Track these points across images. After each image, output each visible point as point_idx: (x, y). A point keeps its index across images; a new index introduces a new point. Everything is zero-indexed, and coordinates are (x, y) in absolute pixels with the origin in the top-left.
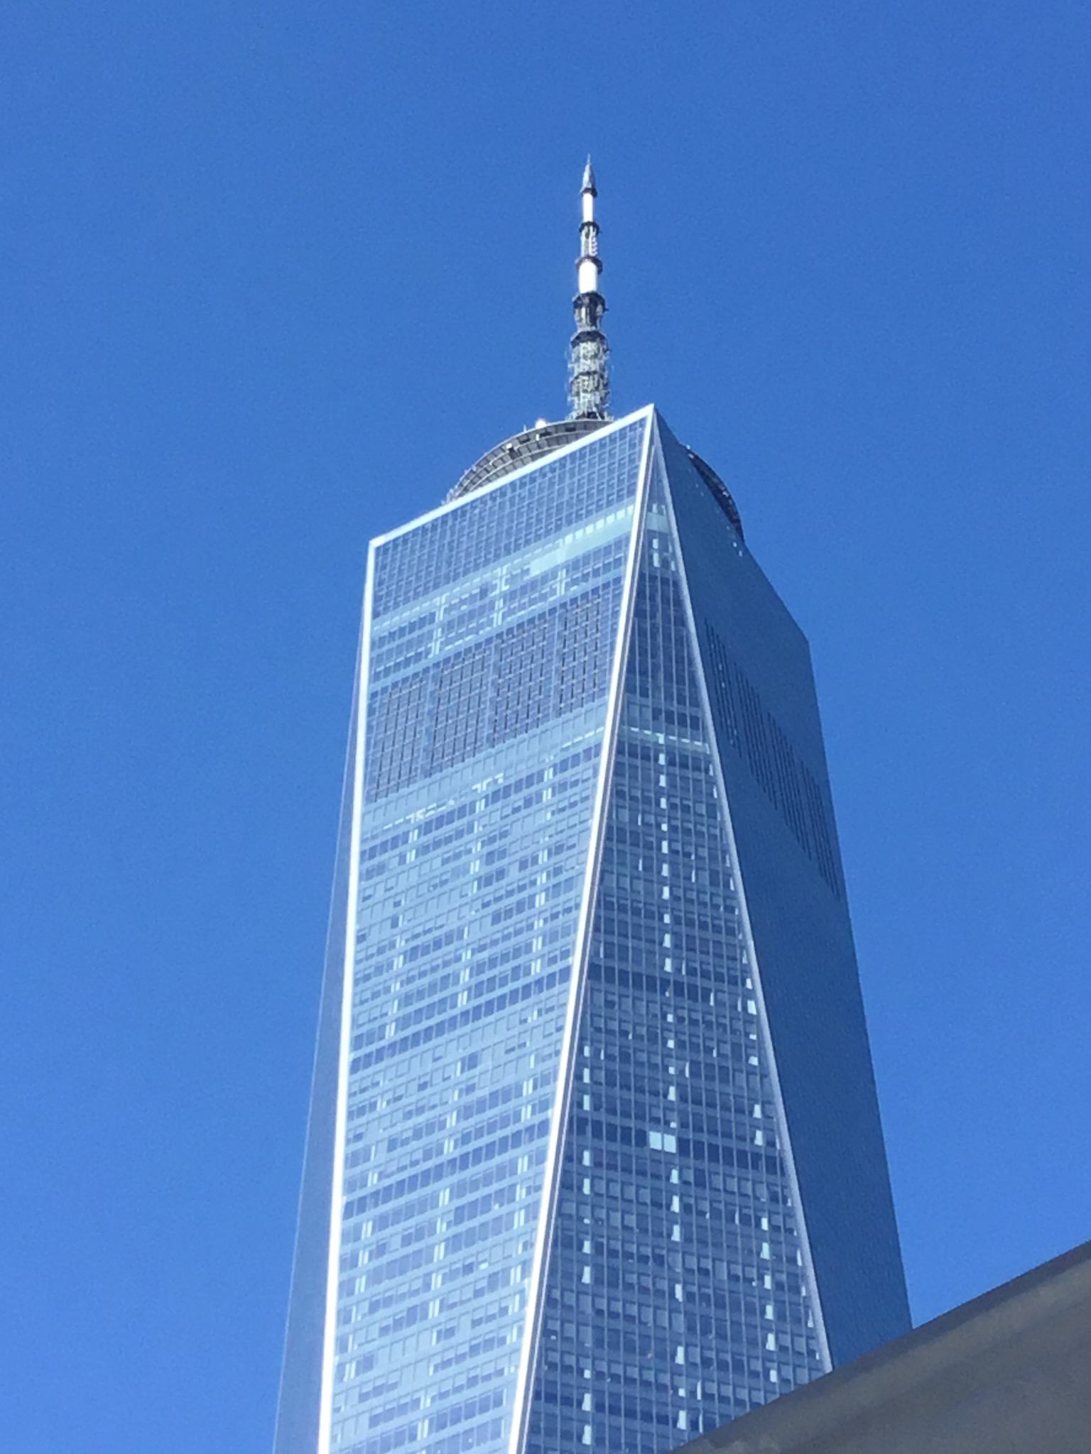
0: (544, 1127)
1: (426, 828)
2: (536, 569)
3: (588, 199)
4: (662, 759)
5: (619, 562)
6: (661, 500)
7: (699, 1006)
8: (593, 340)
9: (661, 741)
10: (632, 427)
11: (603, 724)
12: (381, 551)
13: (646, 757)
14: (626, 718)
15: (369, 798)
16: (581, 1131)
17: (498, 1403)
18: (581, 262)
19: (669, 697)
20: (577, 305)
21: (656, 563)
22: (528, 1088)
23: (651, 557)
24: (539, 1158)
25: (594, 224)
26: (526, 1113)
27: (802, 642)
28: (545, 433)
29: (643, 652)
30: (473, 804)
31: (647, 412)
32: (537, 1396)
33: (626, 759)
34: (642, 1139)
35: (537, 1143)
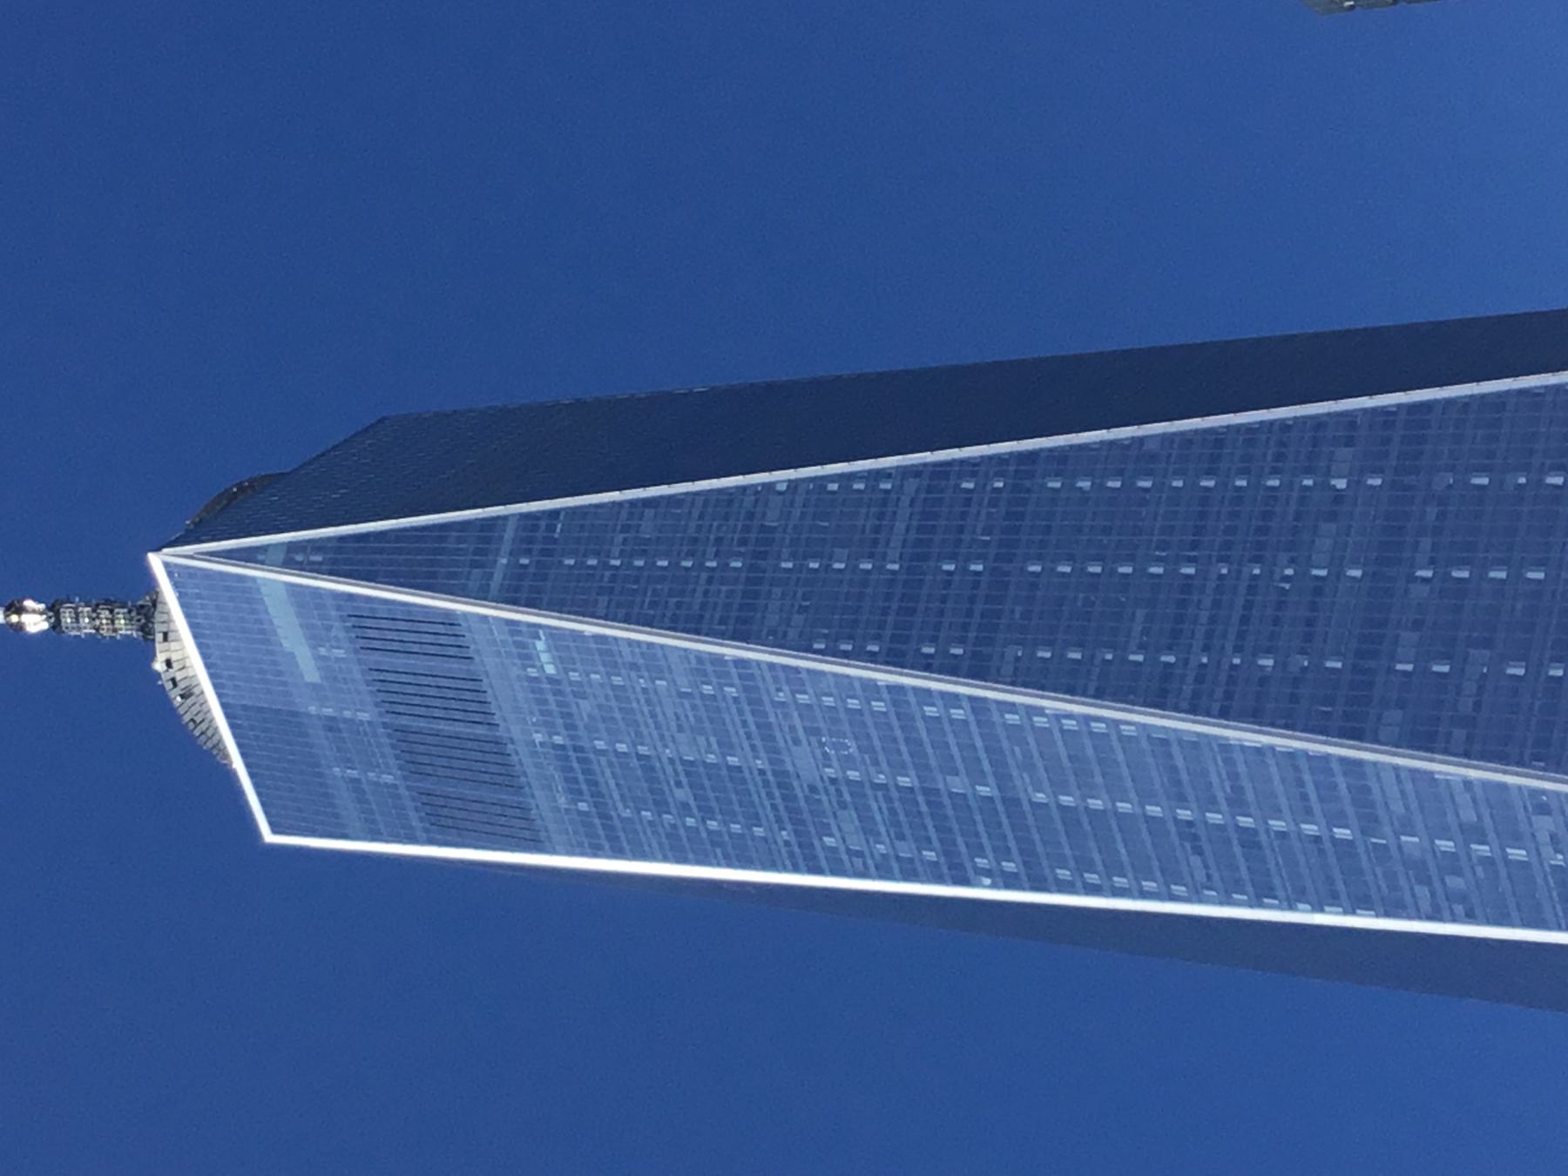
0: (891, 688)
1: (575, 794)
2: (311, 673)
5: (316, 592)
7: (778, 536)
8: (57, 615)
9: (504, 561)
10: (170, 574)
11: (485, 618)
12: (276, 829)
13: (521, 577)
14: (482, 595)
15: (536, 846)
16: (903, 654)
17: (1165, 742)
21: (318, 558)
22: (853, 703)
23: (313, 563)
24: (926, 695)
26: (878, 706)
28: (169, 663)
30: (555, 747)
31: (155, 561)
32: (1162, 707)
33: (524, 596)
35: (912, 699)
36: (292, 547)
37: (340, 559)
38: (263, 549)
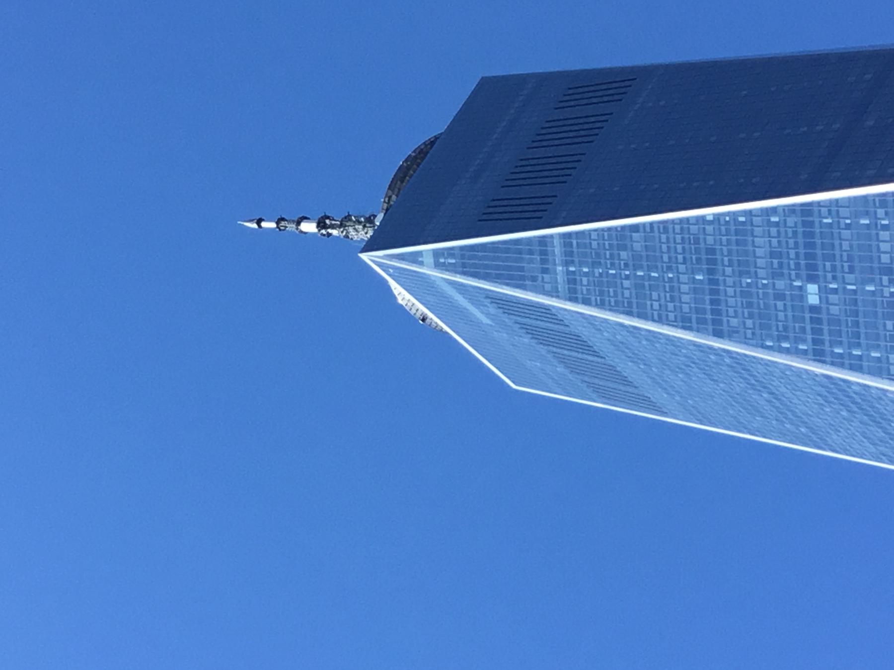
2: (485, 320)
3: (264, 224)
4: (572, 269)
6: (412, 253)
14: (554, 293)
18: (301, 232)
19: (531, 261)
20: (329, 235)
25: (278, 223)
27: (486, 84)
29: (511, 277)
34: (813, 309)
36: (437, 253)
37: (467, 263)
38: (420, 253)
